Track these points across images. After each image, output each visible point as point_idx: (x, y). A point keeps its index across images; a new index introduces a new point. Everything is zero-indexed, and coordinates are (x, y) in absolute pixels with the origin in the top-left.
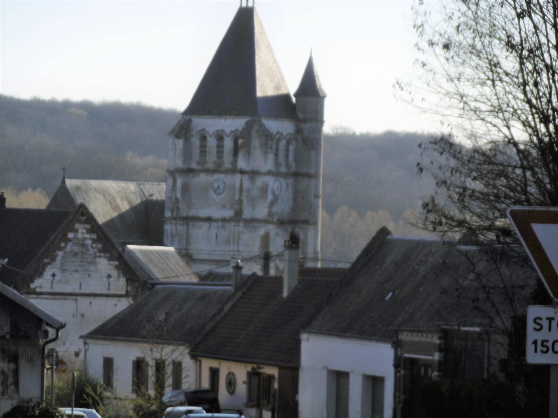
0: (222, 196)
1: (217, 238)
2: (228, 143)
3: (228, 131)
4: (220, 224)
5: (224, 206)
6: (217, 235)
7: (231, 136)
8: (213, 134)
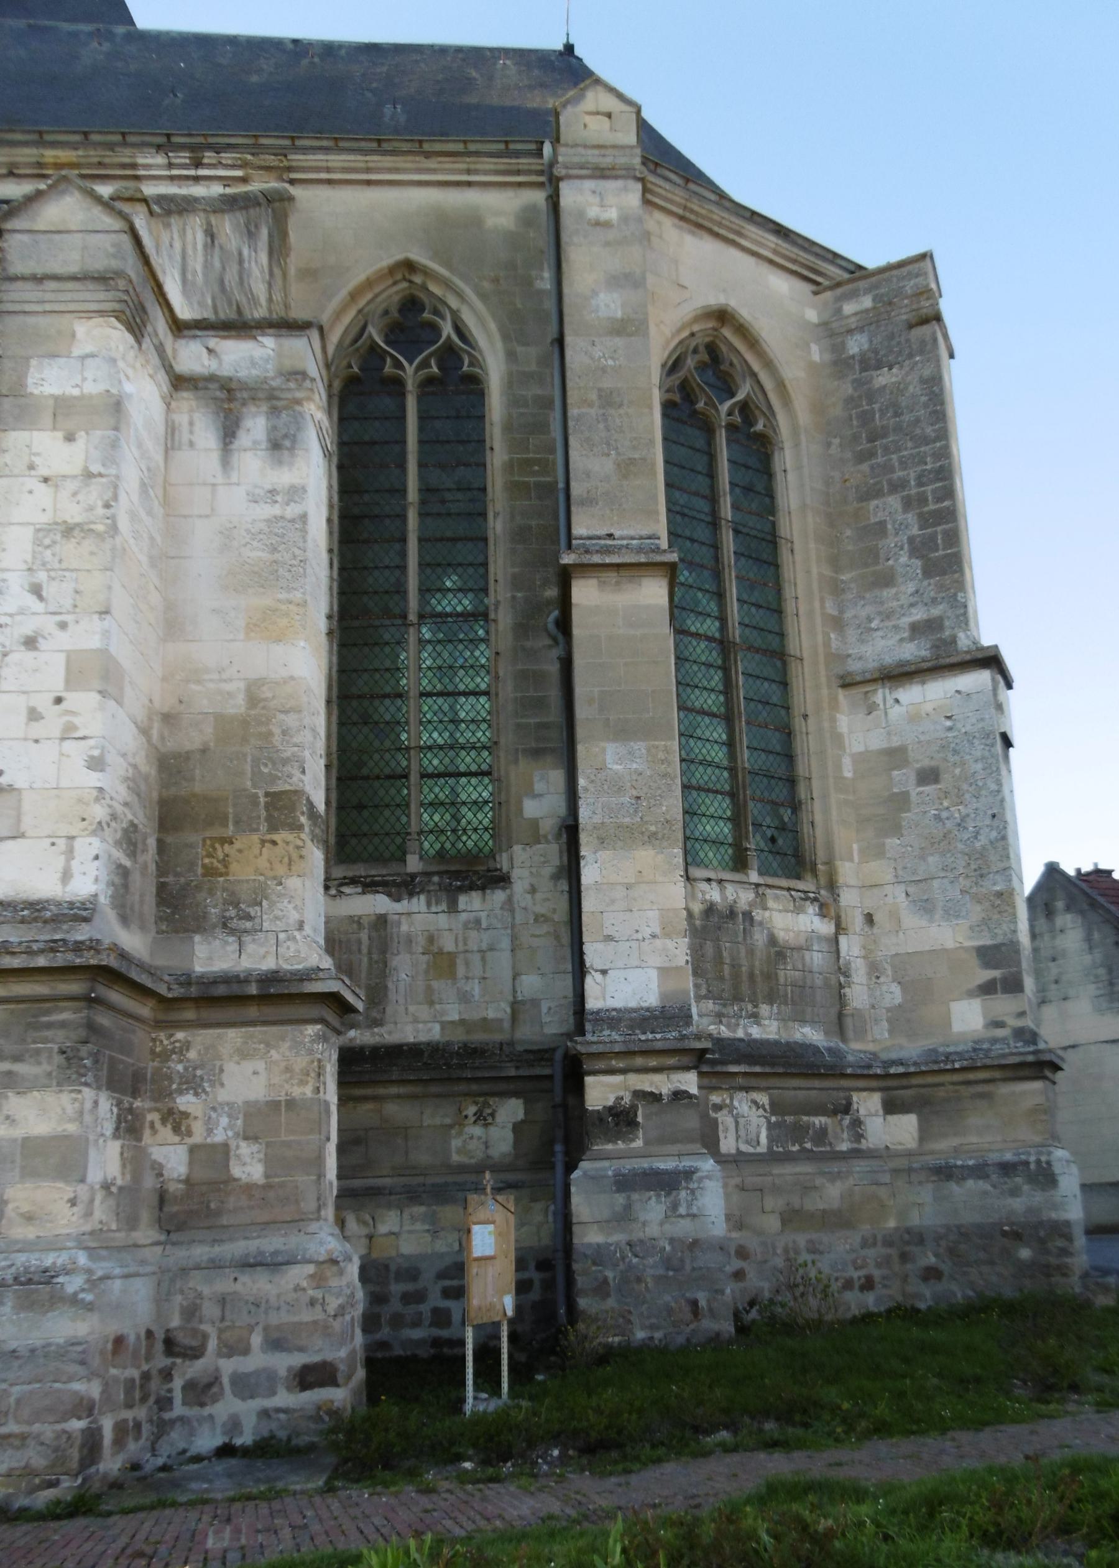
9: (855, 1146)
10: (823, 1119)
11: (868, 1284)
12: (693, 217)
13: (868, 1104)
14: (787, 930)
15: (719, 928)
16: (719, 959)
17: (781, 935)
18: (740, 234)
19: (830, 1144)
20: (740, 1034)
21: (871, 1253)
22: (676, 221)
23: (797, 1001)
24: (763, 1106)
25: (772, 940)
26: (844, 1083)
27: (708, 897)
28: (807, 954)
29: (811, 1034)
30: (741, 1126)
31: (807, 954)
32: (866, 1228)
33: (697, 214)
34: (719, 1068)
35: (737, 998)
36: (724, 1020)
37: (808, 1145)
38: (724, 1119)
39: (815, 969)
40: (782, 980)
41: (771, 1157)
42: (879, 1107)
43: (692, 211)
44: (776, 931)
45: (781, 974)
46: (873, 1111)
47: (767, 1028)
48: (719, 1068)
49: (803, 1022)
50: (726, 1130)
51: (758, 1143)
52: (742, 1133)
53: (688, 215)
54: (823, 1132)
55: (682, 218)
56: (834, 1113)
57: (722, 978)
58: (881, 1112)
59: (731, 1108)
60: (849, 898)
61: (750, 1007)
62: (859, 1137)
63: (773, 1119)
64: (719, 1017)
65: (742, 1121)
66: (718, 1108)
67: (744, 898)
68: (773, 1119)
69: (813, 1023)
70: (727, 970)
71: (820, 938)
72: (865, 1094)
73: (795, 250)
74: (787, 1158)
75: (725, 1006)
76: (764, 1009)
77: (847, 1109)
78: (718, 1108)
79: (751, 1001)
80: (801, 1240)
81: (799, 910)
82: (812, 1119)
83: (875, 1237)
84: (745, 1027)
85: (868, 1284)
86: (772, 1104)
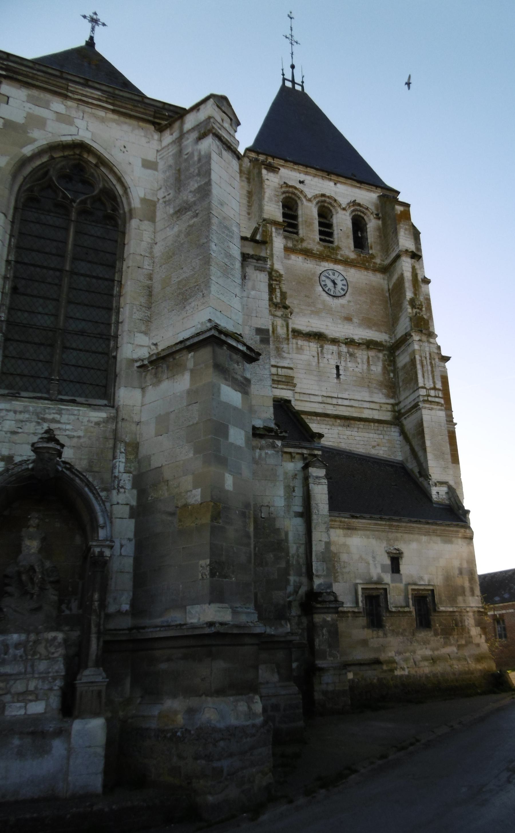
0: (342, 301)
1: (338, 375)
2: (342, 222)
3: (344, 201)
4: (344, 348)
5: (348, 319)
6: (337, 367)
7: (349, 211)
8: (315, 197)
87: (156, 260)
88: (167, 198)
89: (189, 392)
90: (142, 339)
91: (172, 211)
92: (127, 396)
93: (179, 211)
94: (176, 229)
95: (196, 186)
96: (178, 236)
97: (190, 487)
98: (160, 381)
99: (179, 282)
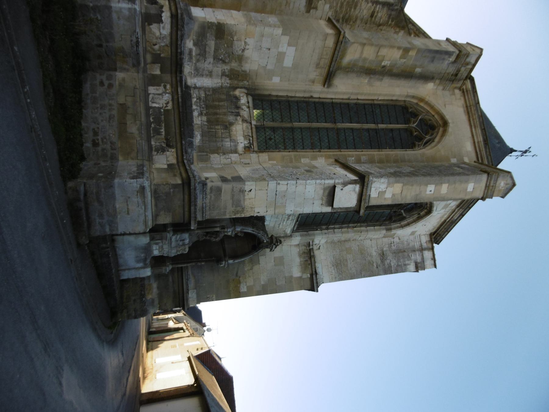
9: (154, 149)
10: (163, 133)
11: (95, 144)
12: (469, 110)
13: (171, 156)
14: (236, 131)
15: (231, 102)
16: (220, 100)
17: (234, 128)
18: (475, 127)
19: (154, 136)
20: (194, 107)
21: (108, 146)
22: (465, 106)
23: (209, 134)
24: (167, 106)
25: (231, 124)
26: (179, 145)
27: (242, 98)
28: (228, 140)
29: (197, 139)
30: (159, 96)
31: (228, 140)
32: (119, 144)
33: (471, 111)
34: (179, 84)
35: (207, 107)
36: (198, 101)
37: (153, 126)
38: (161, 89)
39: (224, 143)
40: (216, 127)
41: (148, 108)
42: (171, 163)
43: (471, 109)
44: (235, 126)
45: (219, 127)
46: (169, 159)
47: (198, 120)
48: (179, 84)
49: (202, 136)
50: (157, 90)
51: (153, 103)
52: (156, 96)
53: (469, 108)
54: (159, 133)
55: (467, 107)
56: (167, 139)
57: (213, 101)
58: (168, 163)
59: (166, 93)
60: (254, 156)
61: (205, 112)
62: (157, 150)
63: (162, 110)
64: (199, 98)
65: (161, 97)
66: (165, 87)
67: (245, 113)
68: (162, 110)
69: (202, 140)
70: (217, 103)
71: (236, 146)
72: (175, 155)
73: (484, 149)
74: (148, 115)
75: (203, 101)
76: (205, 118)
77: (169, 146)
78: (165, 87)
79: (207, 112)
80: (115, 112)
81: (245, 137)
82: (163, 128)
83: (115, 149)
84: (197, 109)
85: (95, 144)
86: (168, 110)
87: (362, 242)
88: (393, 245)
89: (291, 277)
90: (323, 241)
91: (385, 249)
92: (297, 239)
93: (383, 254)
94: (374, 254)
95: (392, 264)
96: (371, 256)
97: (248, 284)
98: (300, 256)
99: (347, 260)
